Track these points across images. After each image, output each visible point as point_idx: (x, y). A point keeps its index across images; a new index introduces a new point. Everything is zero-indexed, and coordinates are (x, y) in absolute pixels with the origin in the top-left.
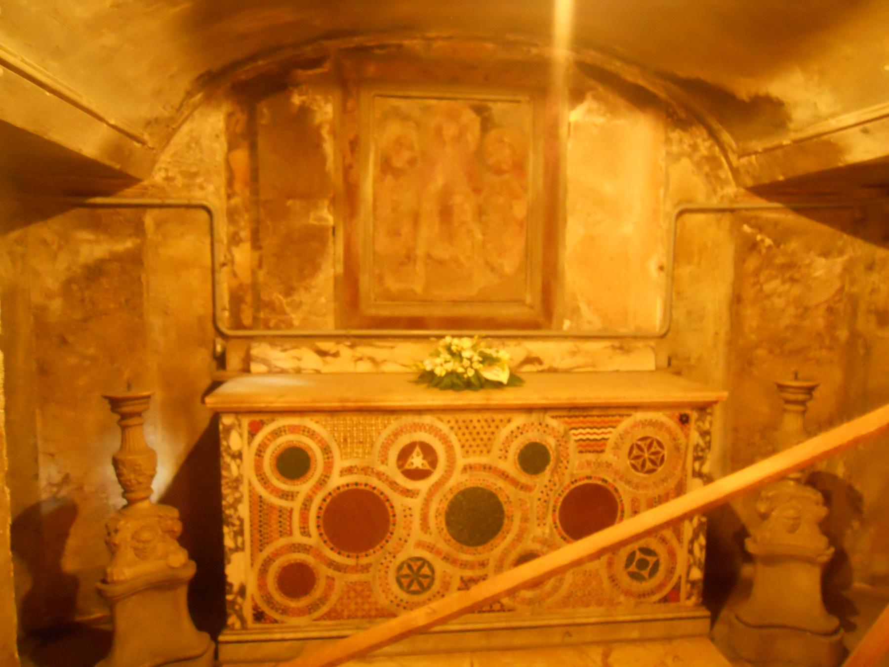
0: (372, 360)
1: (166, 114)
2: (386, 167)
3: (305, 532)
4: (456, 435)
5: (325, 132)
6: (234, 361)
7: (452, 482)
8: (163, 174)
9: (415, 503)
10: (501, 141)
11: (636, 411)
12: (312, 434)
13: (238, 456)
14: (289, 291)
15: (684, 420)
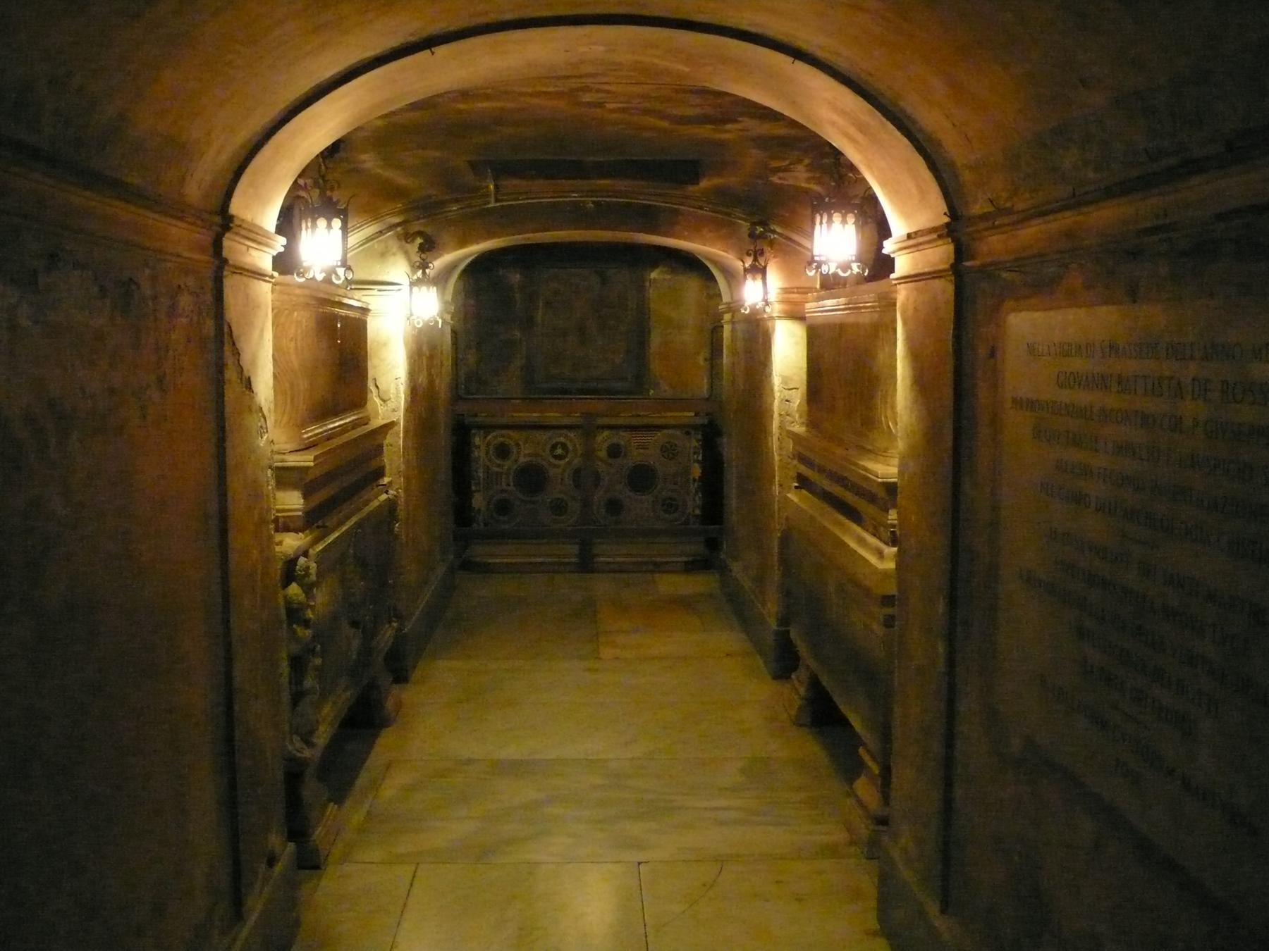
2: (548, 304)
12: (509, 437)
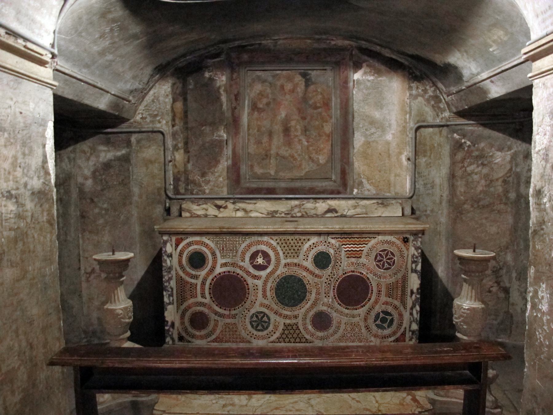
0: (245, 210)
1: (141, 87)
2: (254, 107)
3: (203, 296)
4: (280, 247)
5: (222, 91)
6: (174, 210)
7: (278, 272)
8: (140, 116)
9: (260, 283)
10: (316, 91)
11: (378, 236)
12: (207, 246)
13: (170, 256)
14: (203, 175)
15: (406, 241)
